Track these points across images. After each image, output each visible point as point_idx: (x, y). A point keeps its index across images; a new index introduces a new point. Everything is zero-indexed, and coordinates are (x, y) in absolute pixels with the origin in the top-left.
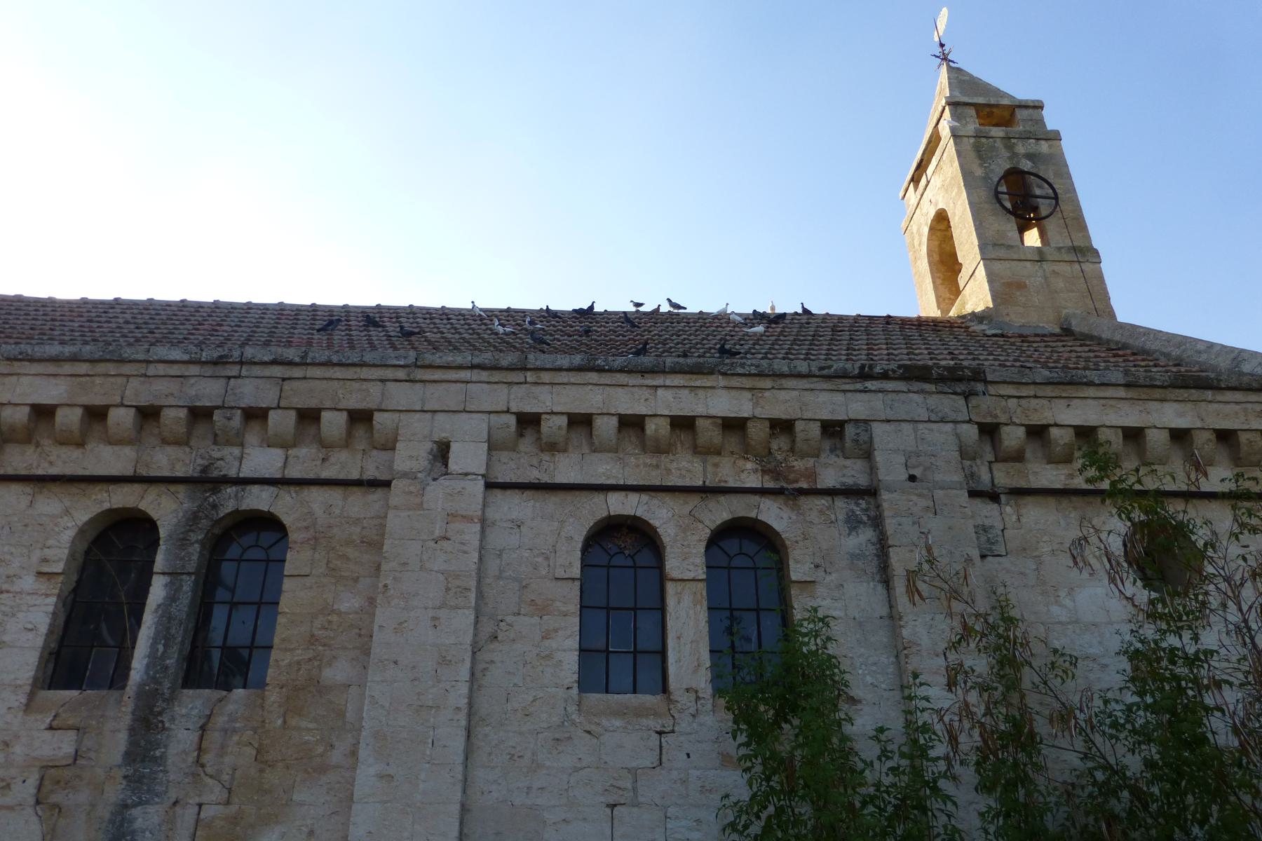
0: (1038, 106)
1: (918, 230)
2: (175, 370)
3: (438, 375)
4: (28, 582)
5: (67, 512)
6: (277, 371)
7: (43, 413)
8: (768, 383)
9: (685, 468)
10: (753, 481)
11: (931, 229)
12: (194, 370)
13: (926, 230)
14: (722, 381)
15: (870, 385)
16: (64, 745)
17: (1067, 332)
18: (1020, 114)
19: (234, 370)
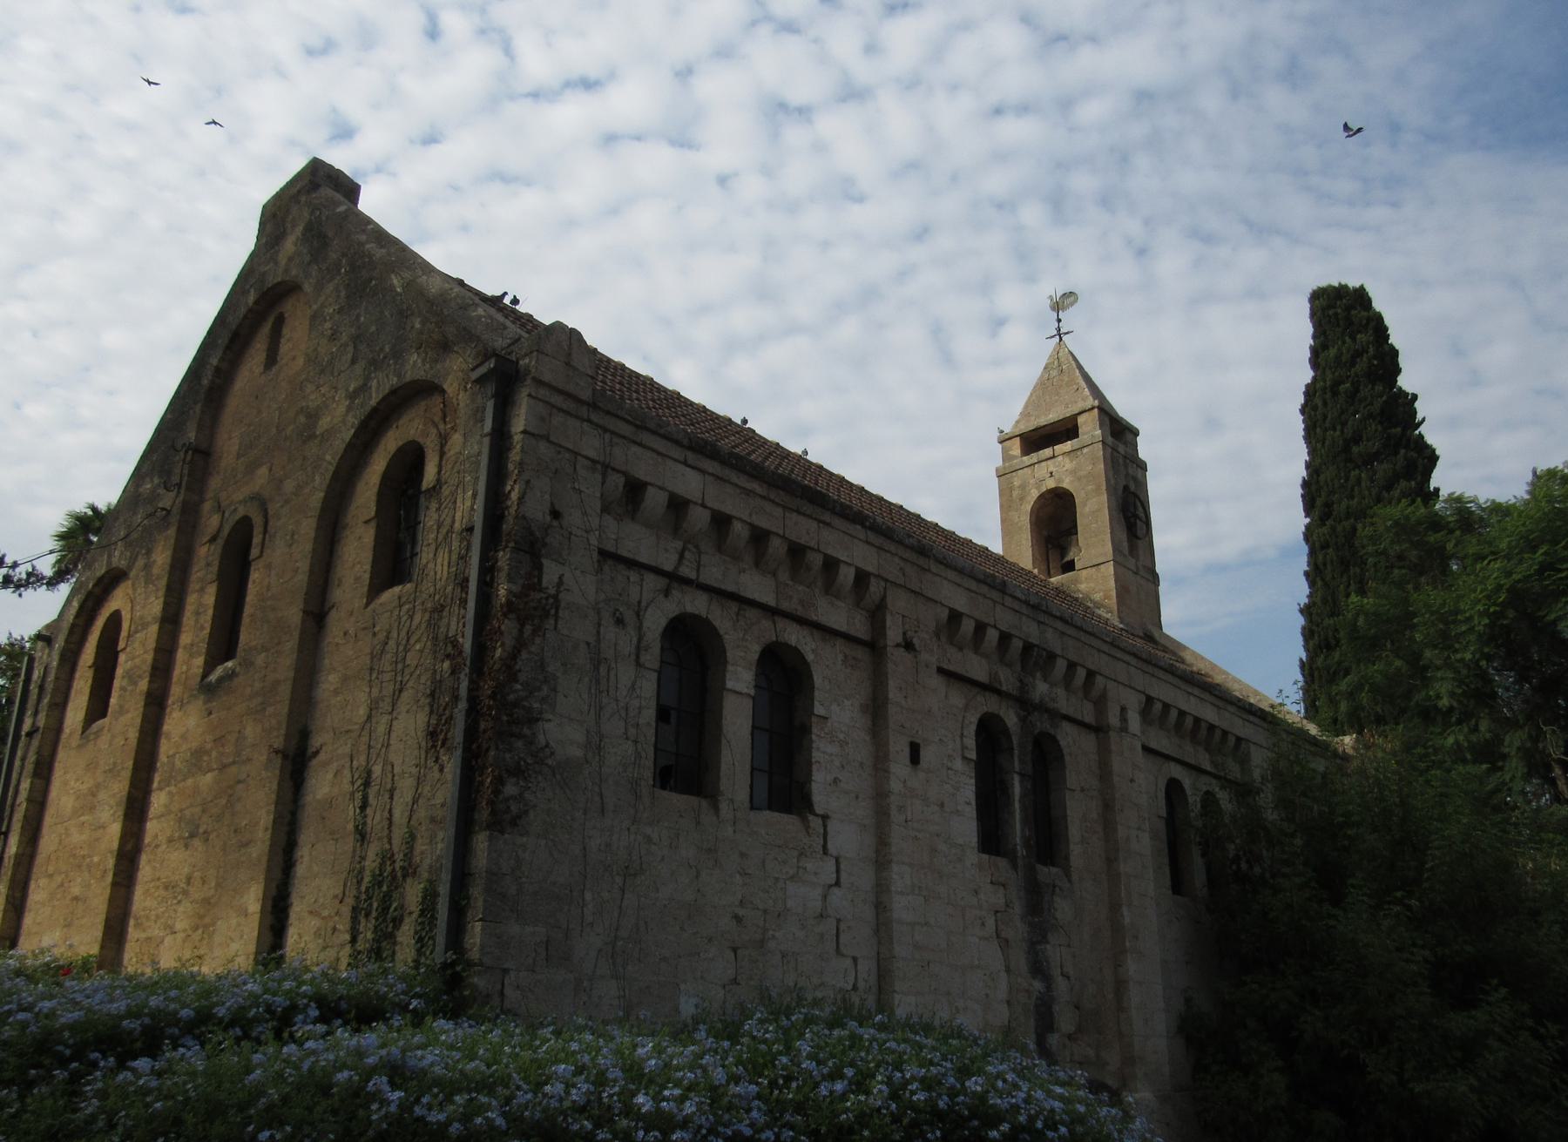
0: (1135, 433)
1: (1023, 487)
2: (1016, 605)
3: (1119, 654)
4: (958, 764)
5: (966, 708)
6: (1059, 625)
7: (955, 617)
8: (1221, 704)
9: (1191, 753)
10: (1207, 766)
11: (1041, 496)
12: (1024, 610)
13: (1035, 494)
14: (1212, 699)
15: (1252, 718)
16: (998, 899)
17: (1149, 638)
18: (1129, 436)
19: (1042, 617)
